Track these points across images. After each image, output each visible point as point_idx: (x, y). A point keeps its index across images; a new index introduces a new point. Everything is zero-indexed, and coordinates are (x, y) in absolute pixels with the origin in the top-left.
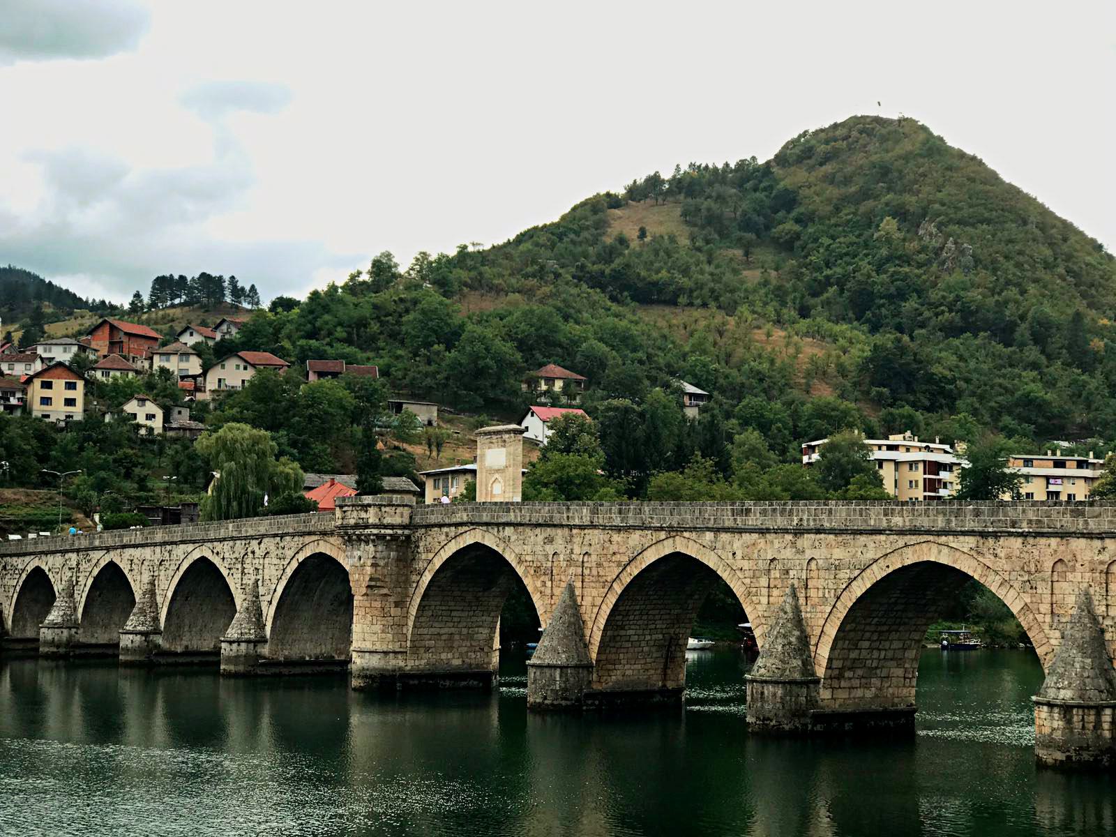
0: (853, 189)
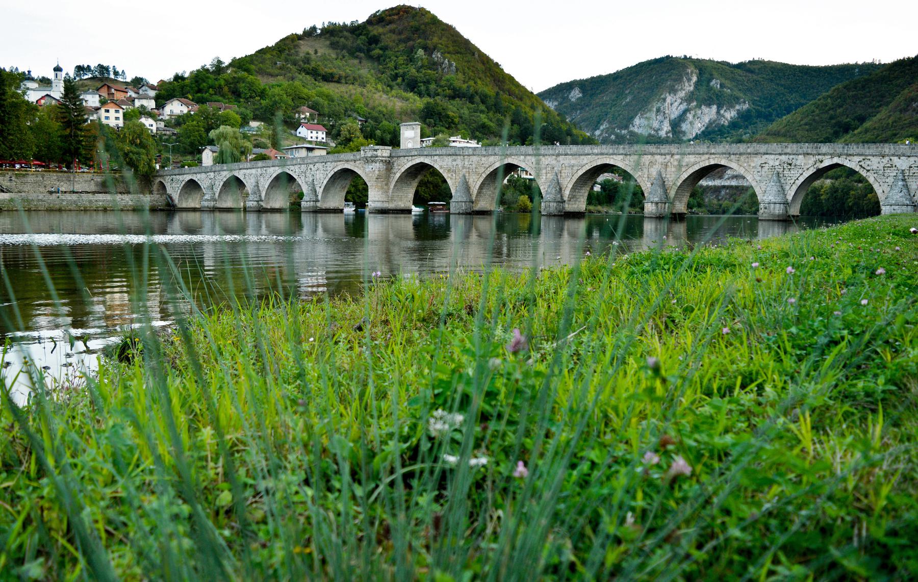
0: (403, 37)
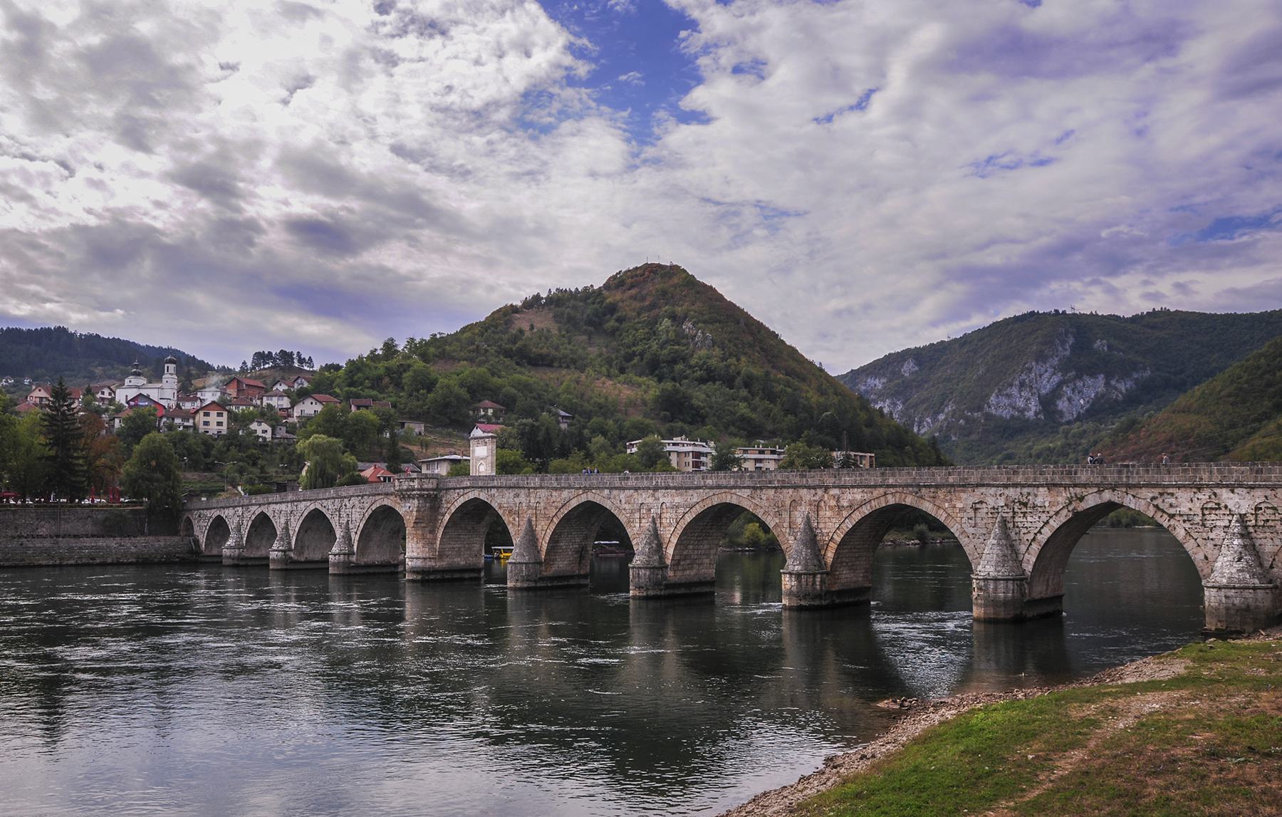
0: (647, 303)
